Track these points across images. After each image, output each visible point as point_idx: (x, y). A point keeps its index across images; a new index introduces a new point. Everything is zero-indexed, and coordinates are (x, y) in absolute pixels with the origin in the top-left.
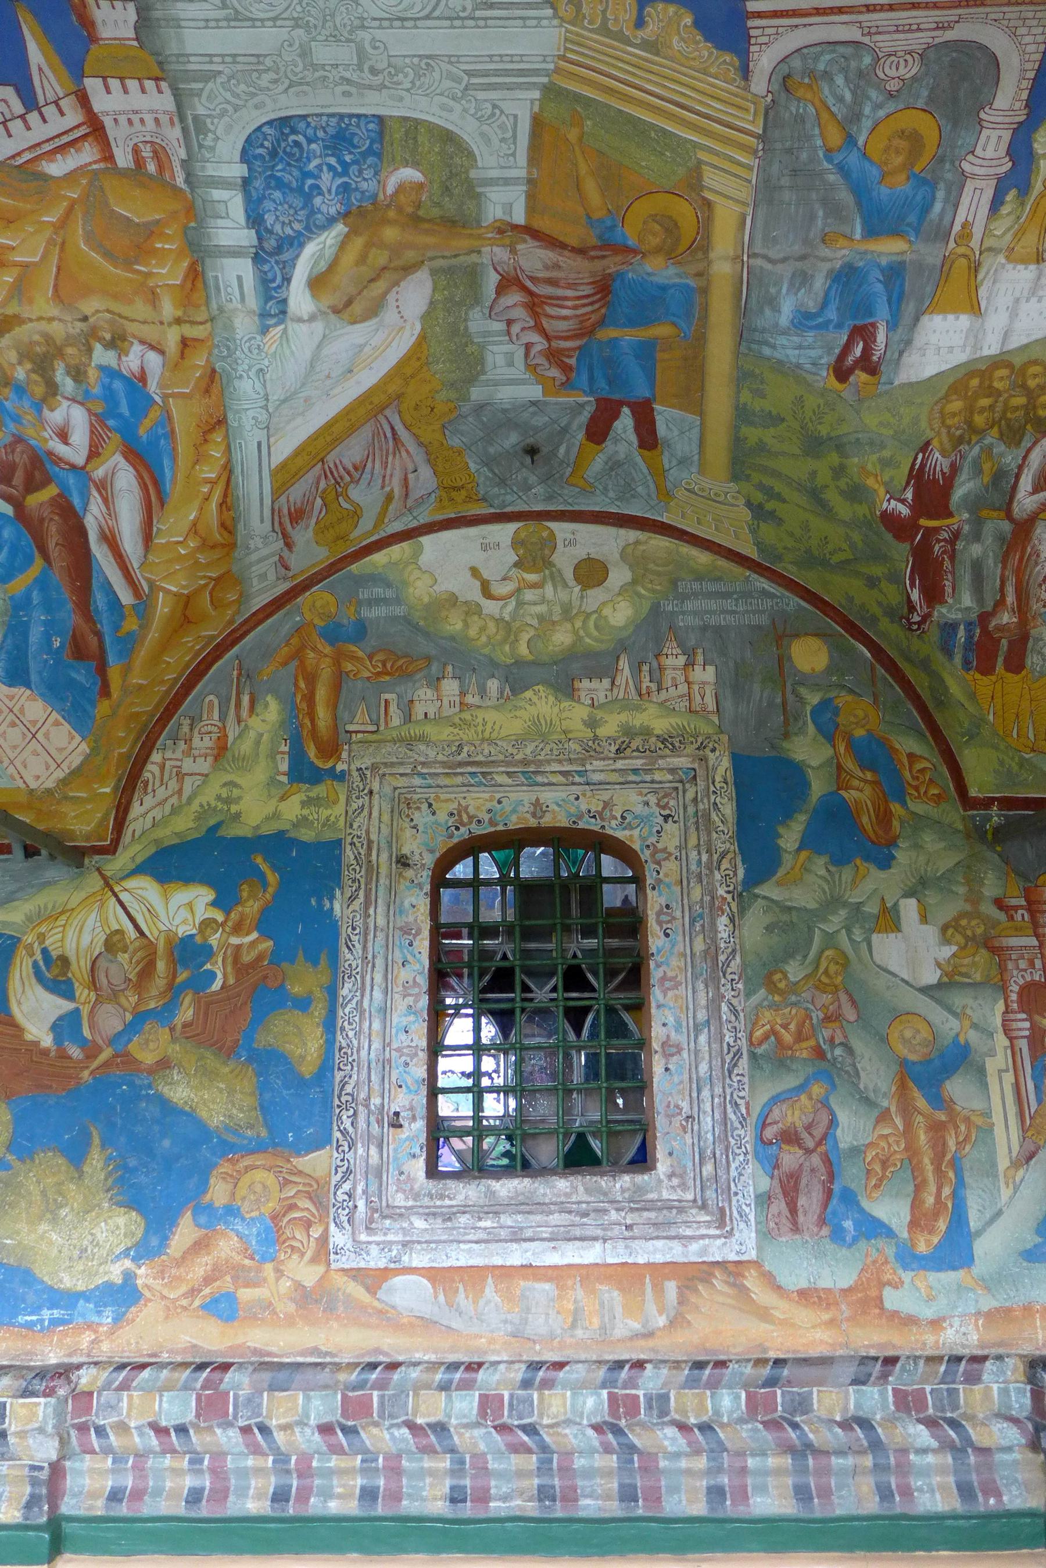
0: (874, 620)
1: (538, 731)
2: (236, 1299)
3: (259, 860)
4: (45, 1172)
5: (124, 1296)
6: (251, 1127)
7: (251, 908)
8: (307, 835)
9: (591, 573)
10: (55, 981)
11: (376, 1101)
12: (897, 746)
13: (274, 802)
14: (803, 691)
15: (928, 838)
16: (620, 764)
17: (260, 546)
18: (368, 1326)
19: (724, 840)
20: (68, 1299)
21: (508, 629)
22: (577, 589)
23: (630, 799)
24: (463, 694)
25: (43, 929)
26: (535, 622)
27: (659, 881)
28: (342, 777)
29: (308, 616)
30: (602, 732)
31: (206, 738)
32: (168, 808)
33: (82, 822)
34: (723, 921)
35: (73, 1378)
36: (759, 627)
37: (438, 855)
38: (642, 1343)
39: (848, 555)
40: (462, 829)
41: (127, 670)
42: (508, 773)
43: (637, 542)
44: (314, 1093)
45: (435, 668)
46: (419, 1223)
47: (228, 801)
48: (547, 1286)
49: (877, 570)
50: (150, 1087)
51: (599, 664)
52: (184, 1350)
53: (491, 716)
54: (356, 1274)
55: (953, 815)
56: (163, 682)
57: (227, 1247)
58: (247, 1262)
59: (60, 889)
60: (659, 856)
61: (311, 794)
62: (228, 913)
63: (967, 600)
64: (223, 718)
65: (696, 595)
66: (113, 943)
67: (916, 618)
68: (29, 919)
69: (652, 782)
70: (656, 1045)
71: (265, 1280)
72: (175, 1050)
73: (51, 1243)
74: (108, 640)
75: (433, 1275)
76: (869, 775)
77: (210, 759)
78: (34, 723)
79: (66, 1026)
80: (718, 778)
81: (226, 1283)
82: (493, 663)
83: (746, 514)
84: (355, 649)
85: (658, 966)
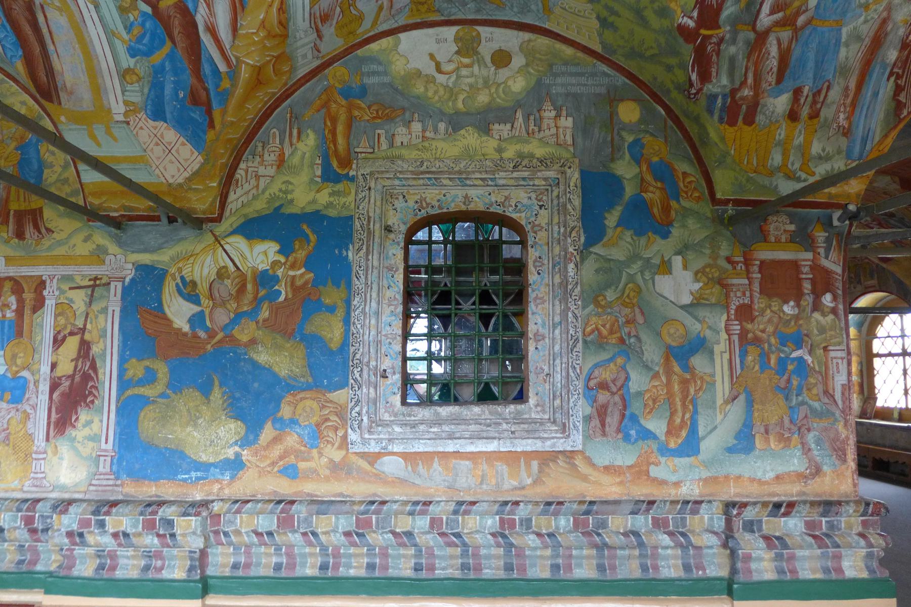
0: (668, 91)
1: (468, 154)
3: (305, 227)
4: (190, 399)
5: (236, 465)
6: (303, 376)
7: (301, 254)
8: (332, 213)
9: (502, 59)
10: (189, 294)
11: (373, 363)
12: (677, 168)
13: (313, 194)
14: (624, 134)
15: (691, 222)
16: (515, 175)
17: (303, 36)
18: (369, 482)
19: (574, 220)
20: (205, 467)
21: (452, 93)
22: (493, 69)
23: (521, 195)
24: (424, 131)
25: (180, 265)
26: (467, 88)
27: (535, 243)
28: (352, 179)
29: (332, 82)
30: (506, 155)
31: (272, 155)
32: (250, 197)
33: (201, 202)
34: (571, 266)
35: (210, 507)
36: (600, 94)
37: (408, 226)
38: (518, 492)
39: (656, 51)
40: (423, 211)
41: (224, 113)
42: (450, 179)
43: (530, 41)
44: (338, 359)
45: (407, 115)
46: (397, 429)
47: (286, 192)
48: (467, 463)
49: (673, 61)
51: (505, 115)
52: (270, 494)
53: (441, 145)
54: (363, 455)
55: (707, 209)
56: (245, 120)
57: (291, 440)
58: (303, 448)
59: (188, 242)
60: (536, 229)
61: (335, 189)
62: (287, 257)
63: (725, 81)
64: (282, 142)
65: (563, 74)
66: (221, 274)
67: (693, 91)
68: (172, 259)
69: (534, 185)
70: (530, 335)
71: (313, 458)
72: (259, 334)
73: (194, 437)
74: (212, 94)
75: (405, 456)
76: (659, 184)
77: (275, 167)
78: (170, 143)
79: (196, 320)
80: (572, 184)
81: (292, 459)
82: (442, 113)
83: (596, 24)
84: (359, 102)
85: (533, 291)
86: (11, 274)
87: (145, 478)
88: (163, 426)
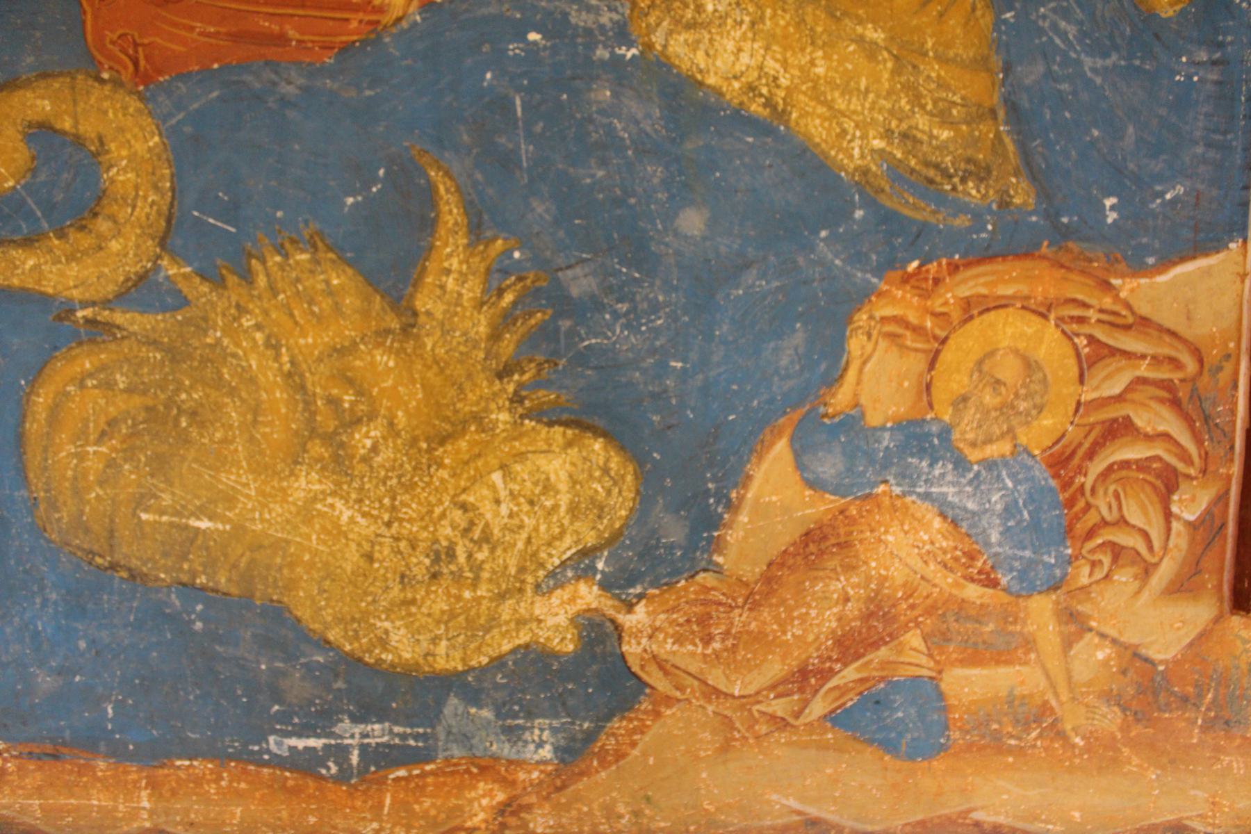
2: (941, 696)
6: (981, 173)
50: (622, 34)
58: (973, 592)
71: (1029, 644)
73: (337, 532)
87: (91, 742)
88: (160, 464)
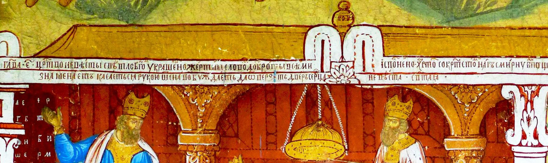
86: (405, 80)
